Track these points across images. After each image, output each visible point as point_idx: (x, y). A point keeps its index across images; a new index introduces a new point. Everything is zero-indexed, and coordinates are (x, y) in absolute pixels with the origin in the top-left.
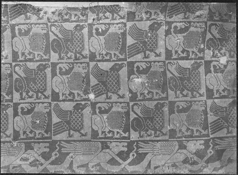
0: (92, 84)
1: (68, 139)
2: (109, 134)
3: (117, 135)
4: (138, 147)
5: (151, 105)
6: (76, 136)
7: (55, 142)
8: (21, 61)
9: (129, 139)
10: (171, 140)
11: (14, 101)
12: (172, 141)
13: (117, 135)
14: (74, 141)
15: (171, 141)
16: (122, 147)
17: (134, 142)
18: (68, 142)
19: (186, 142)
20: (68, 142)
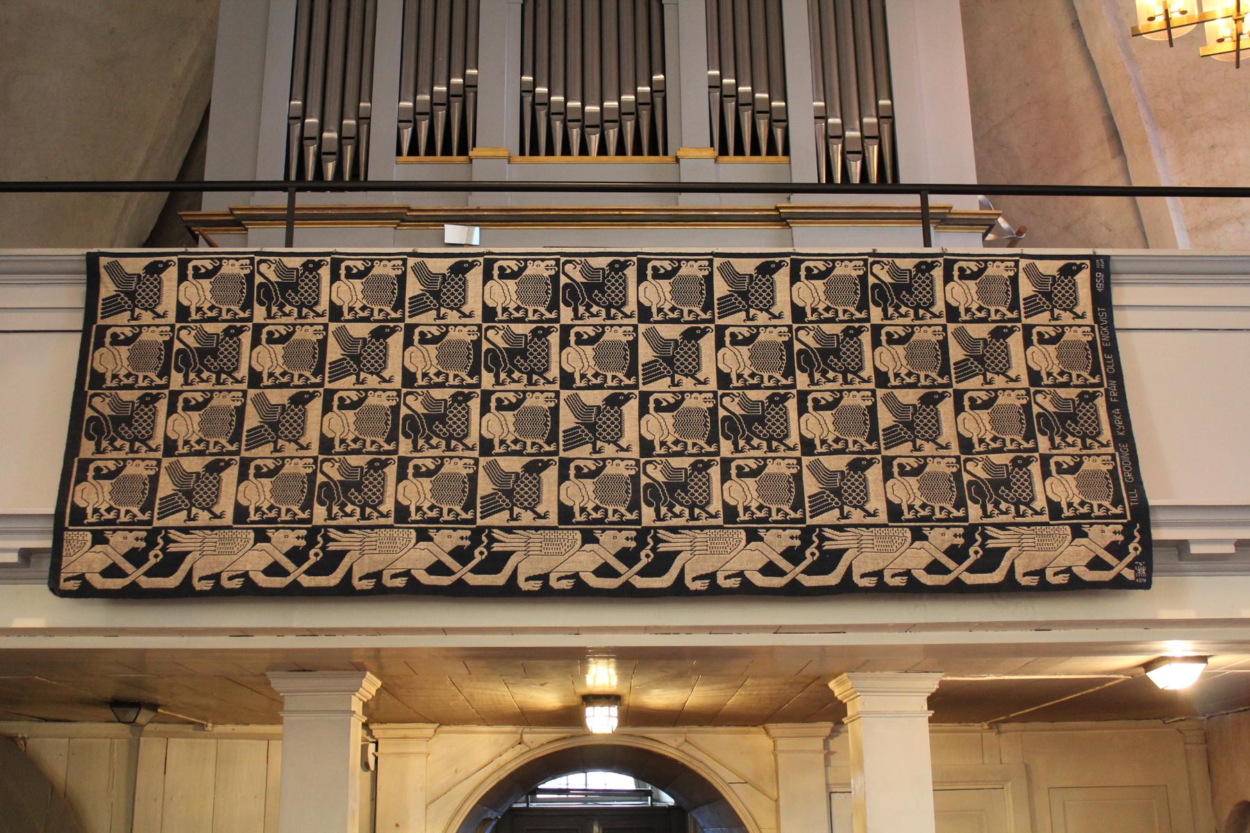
0: (563, 426)
1: (508, 525)
2: (597, 513)
3: (613, 516)
4: (657, 541)
5: (684, 463)
6: (527, 518)
7: (482, 529)
8: (420, 387)
9: (640, 524)
10: (728, 526)
11: (401, 453)
12: (730, 528)
13: (613, 516)
14: (525, 528)
15: (726, 528)
16: (624, 539)
17: (647, 530)
18: (508, 530)
19: (764, 530)
20: (508, 530)
